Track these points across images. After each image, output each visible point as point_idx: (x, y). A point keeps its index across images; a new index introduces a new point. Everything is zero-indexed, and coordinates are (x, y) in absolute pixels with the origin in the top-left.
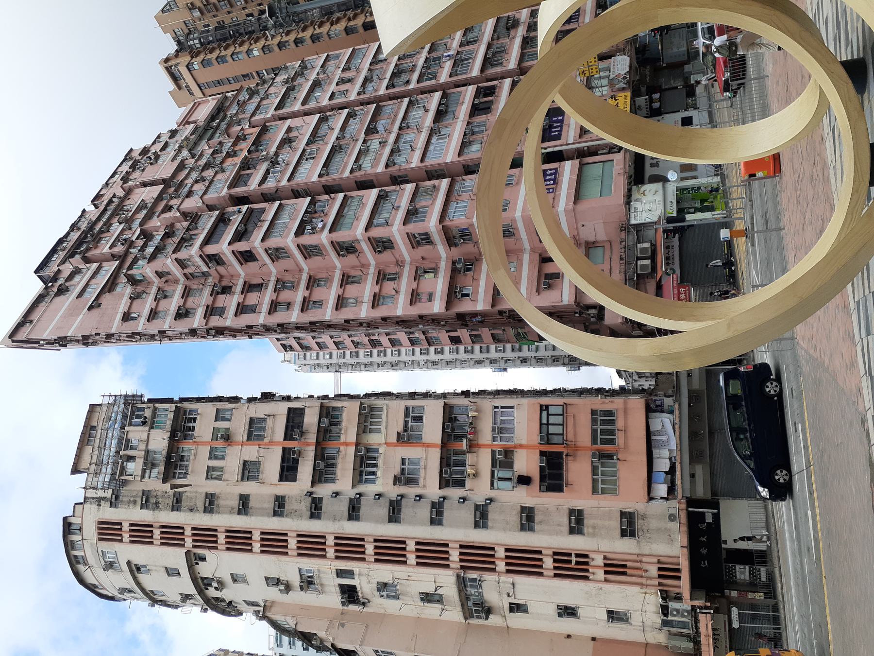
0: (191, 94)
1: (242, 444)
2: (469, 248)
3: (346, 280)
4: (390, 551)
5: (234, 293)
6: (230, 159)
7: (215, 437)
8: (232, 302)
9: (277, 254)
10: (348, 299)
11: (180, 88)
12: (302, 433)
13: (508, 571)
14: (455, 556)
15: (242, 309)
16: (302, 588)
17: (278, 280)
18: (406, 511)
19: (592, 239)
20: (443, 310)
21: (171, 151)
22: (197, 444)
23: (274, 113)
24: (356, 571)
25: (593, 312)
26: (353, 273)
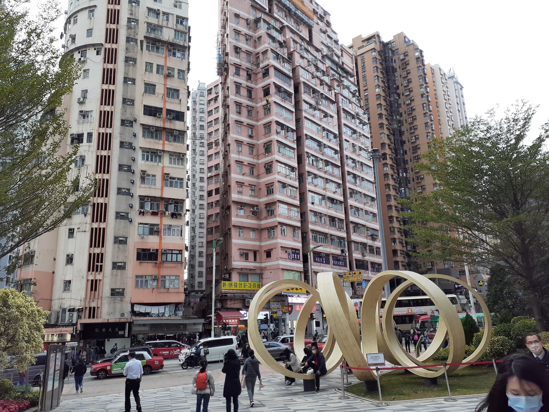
0: (359, 48)
1: (165, 85)
2: (264, 214)
3: (252, 146)
5: (247, 81)
6: (319, 82)
7: (169, 68)
8: (242, 80)
9: (267, 109)
10: (241, 146)
11: (363, 41)
13: (92, 229)
15: (238, 86)
16: (81, 112)
17: (253, 107)
18: (125, 175)
19: (264, 276)
20: (233, 199)
21: (328, 41)
22: (166, 58)
23: (342, 107)
25: (227, 276)
26: (255, 150)
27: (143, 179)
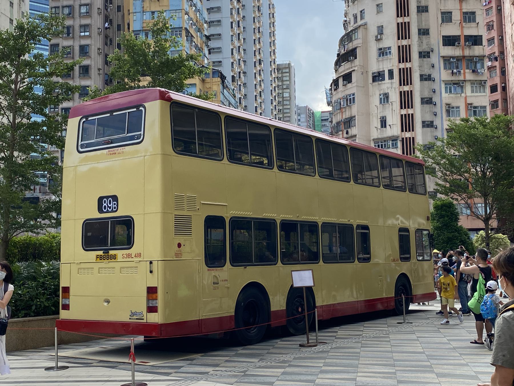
4: (406, 100)
12: (469, 47)
14: (408, 135)
16: (380, 49)
18: (427, 107)
24: (394, 81)
27: (448, 112)
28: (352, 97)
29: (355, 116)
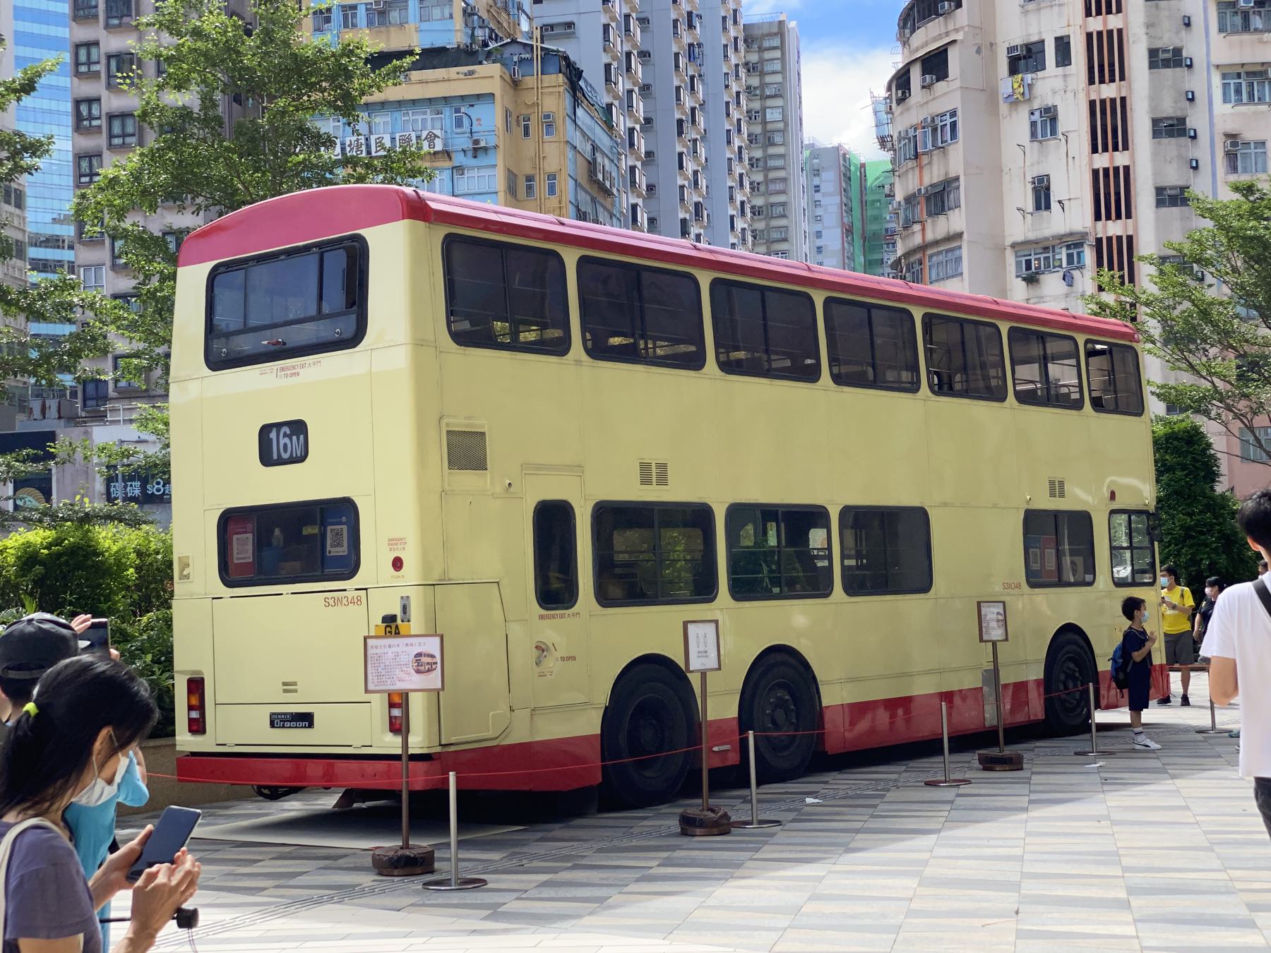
4: (1108, 127)
14: (1114, 228)
18: (1171, 144)
28: (949, 121)
29: (957, 179)
